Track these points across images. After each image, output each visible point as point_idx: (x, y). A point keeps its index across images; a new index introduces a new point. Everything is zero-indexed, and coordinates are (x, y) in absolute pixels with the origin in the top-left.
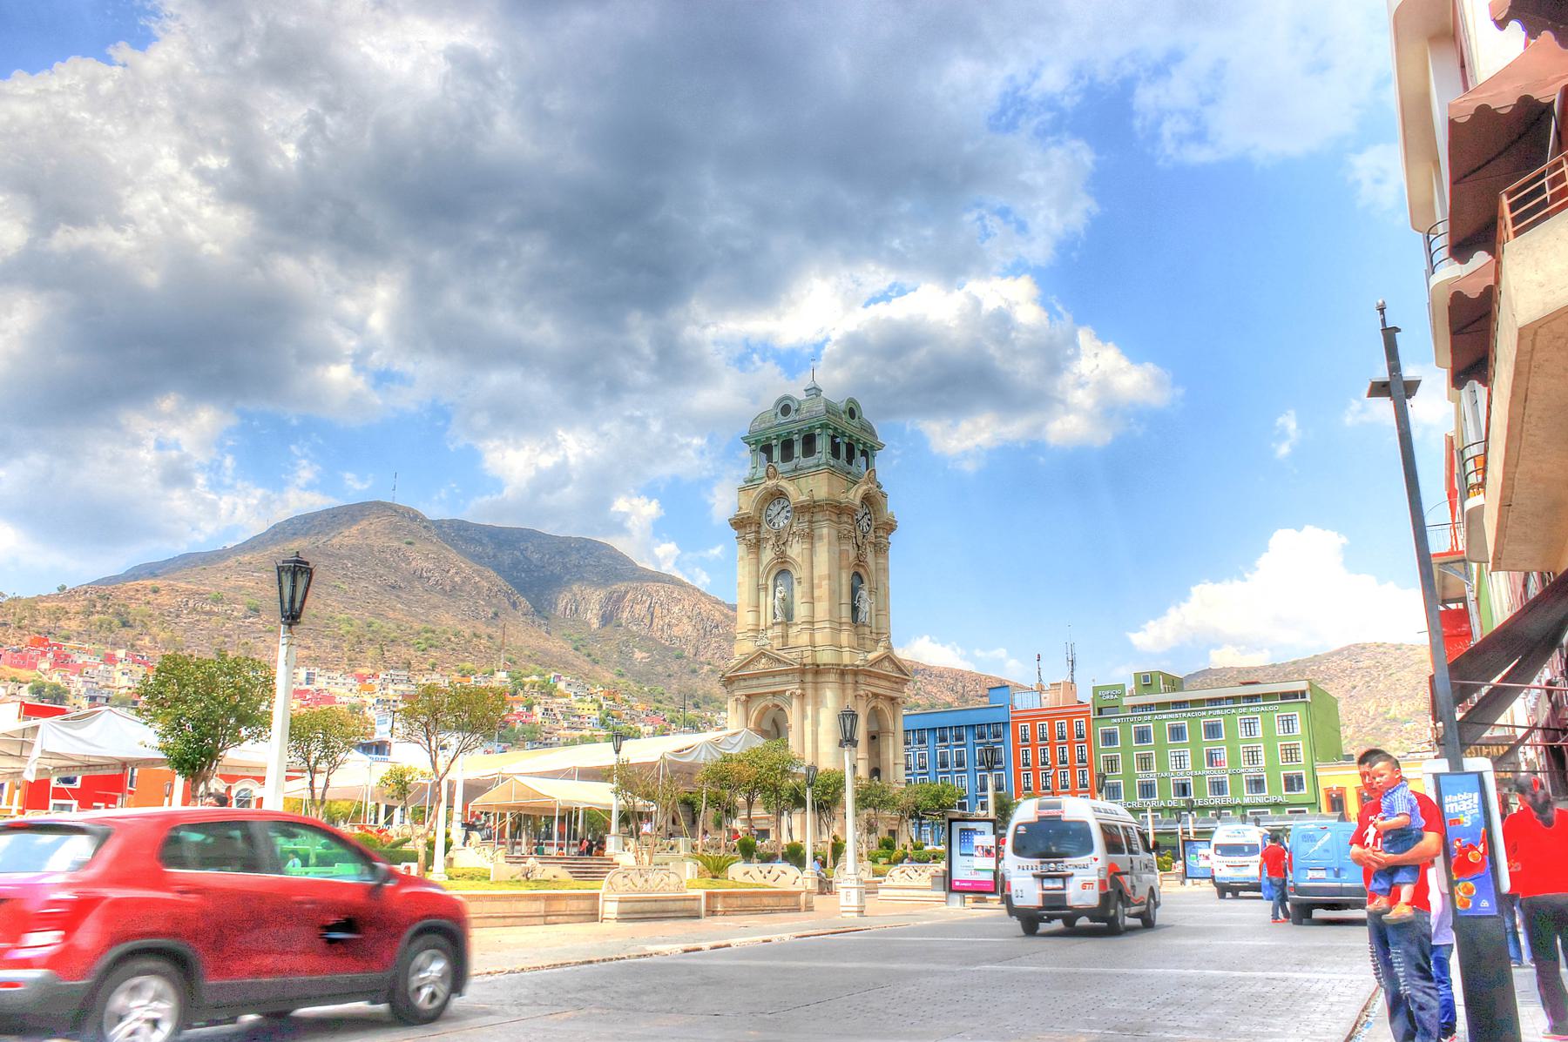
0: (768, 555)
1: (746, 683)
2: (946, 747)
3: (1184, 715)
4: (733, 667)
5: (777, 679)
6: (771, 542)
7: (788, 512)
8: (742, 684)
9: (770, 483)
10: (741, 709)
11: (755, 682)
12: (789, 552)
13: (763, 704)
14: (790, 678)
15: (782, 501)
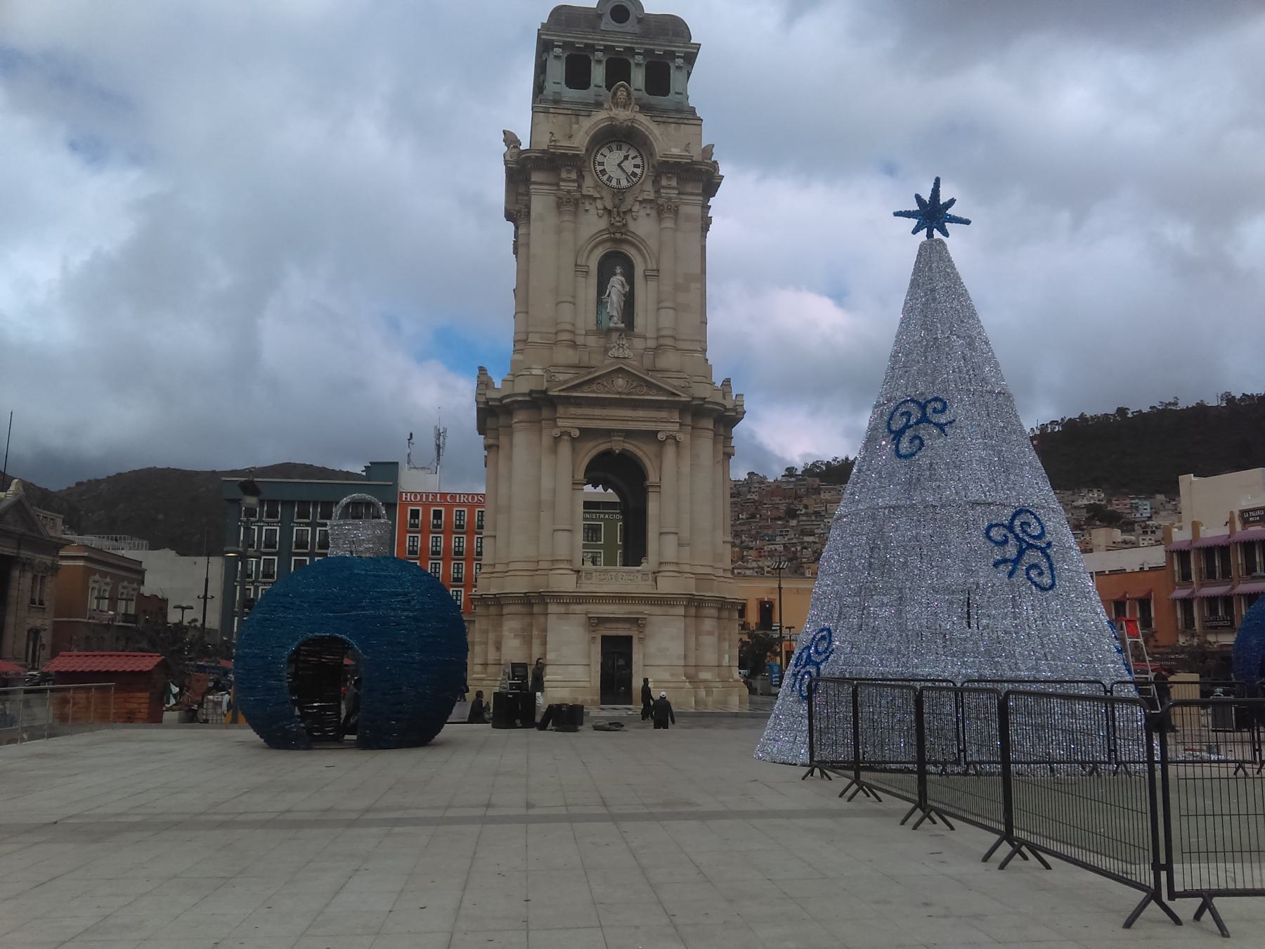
0: (593, 223)
1: (580, 411)
2: (307, 525)
3: (602, 516)
4: (565, 382)
5: (641, 413)
6: (599, 204)
7: (636, 166)
8: (573, 410)
9: (622, 115)
10: (565, 449)
11: (598, 412)
12: (632, 226)
13: (603, 447)
14: (664, 414)
15: (625, 147)
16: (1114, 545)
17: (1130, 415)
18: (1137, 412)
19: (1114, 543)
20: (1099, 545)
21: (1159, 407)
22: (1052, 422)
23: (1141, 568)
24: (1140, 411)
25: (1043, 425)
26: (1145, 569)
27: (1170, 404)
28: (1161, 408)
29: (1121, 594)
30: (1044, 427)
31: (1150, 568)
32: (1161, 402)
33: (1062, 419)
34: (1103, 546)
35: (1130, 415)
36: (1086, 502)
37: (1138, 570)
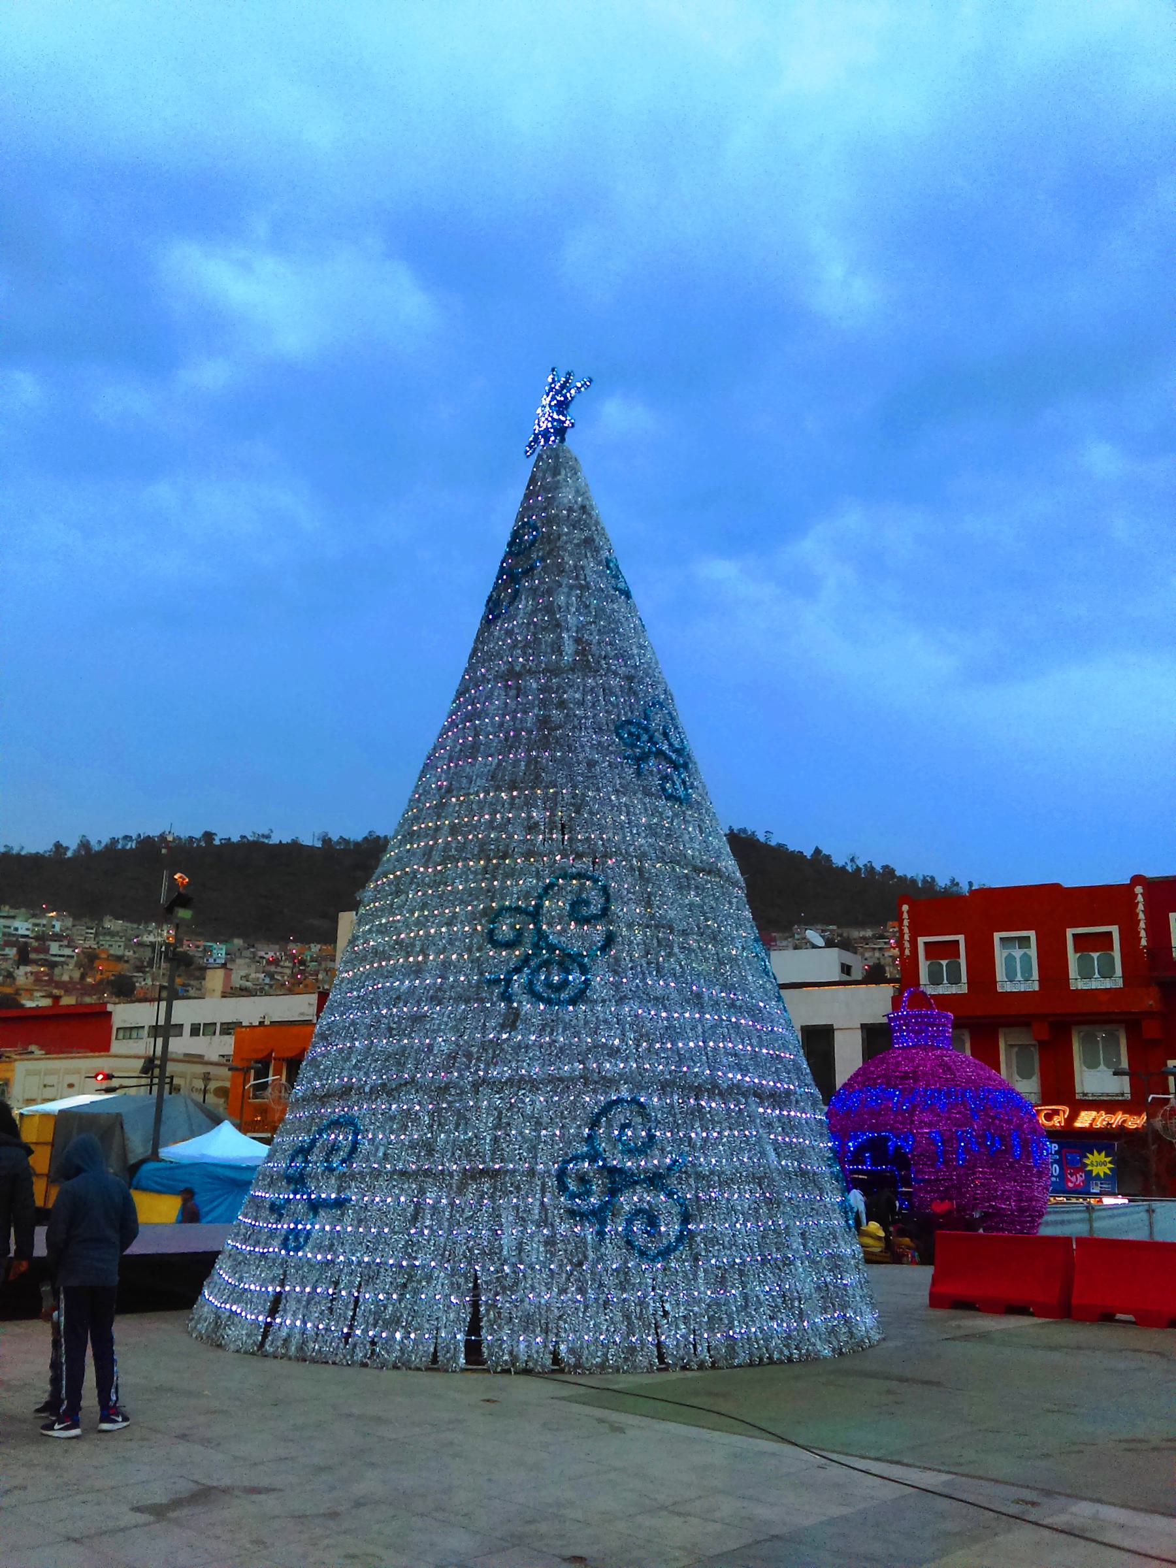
16: (233, 992)
17: (217, 842)
18: (225, 839)
19: (232, 988)
20: (214, 990)
21: (250, 838)
22: (127, 838)
23: (260, 1022)
24: (230, 839)
25: (114, 838)
26: (266, 1023)
27: (264, 836)
28: (251, 839)
29: (265, 1053)
30: (114, 841)
31: (271, 1022)
32: (254, 833)
33: (139, 835)
34: (218, 993)
35: (217, 842)
36: (151, 938)
37: (257, 1024)
